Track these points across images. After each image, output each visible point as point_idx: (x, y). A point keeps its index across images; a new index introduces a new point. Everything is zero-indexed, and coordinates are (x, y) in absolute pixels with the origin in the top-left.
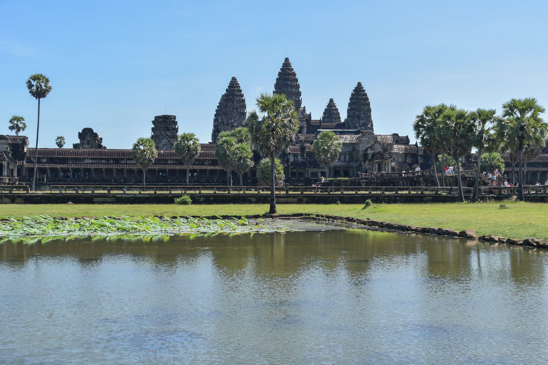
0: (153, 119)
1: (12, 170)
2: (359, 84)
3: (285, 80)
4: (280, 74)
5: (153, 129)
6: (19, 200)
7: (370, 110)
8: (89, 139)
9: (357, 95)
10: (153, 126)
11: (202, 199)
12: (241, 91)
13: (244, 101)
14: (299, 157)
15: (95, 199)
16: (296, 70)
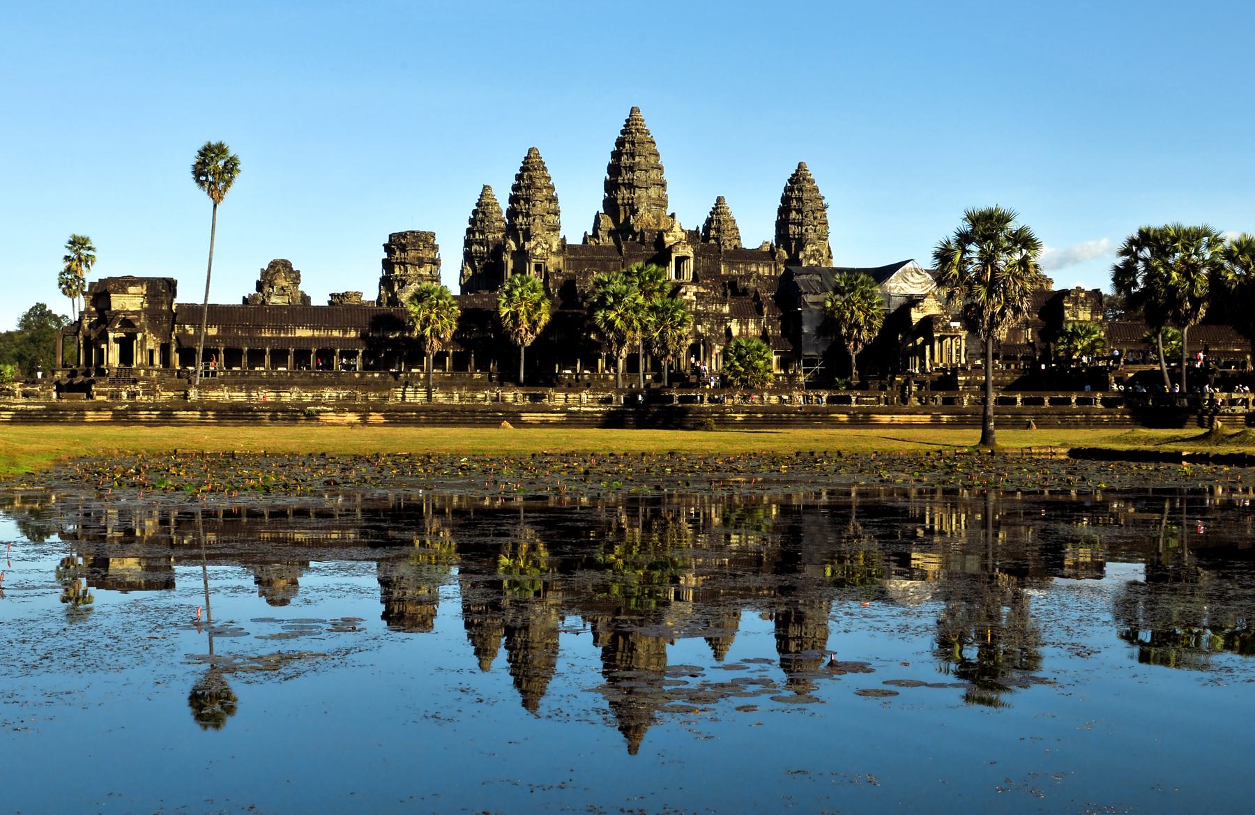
0: (387, 242)
1: (151, 352)
2: (801, 166)
3: (632, 155)
4: (620, 143)
5: (388, 265)
6: (375, 417)
7: (826, 223)
8: (284, 284)
9: (800, 190)
10: (385, 256)
11: (739, 417)
13: (554, 200)
14: (752, 326)
15: (526, 417)
16: (655, 134)
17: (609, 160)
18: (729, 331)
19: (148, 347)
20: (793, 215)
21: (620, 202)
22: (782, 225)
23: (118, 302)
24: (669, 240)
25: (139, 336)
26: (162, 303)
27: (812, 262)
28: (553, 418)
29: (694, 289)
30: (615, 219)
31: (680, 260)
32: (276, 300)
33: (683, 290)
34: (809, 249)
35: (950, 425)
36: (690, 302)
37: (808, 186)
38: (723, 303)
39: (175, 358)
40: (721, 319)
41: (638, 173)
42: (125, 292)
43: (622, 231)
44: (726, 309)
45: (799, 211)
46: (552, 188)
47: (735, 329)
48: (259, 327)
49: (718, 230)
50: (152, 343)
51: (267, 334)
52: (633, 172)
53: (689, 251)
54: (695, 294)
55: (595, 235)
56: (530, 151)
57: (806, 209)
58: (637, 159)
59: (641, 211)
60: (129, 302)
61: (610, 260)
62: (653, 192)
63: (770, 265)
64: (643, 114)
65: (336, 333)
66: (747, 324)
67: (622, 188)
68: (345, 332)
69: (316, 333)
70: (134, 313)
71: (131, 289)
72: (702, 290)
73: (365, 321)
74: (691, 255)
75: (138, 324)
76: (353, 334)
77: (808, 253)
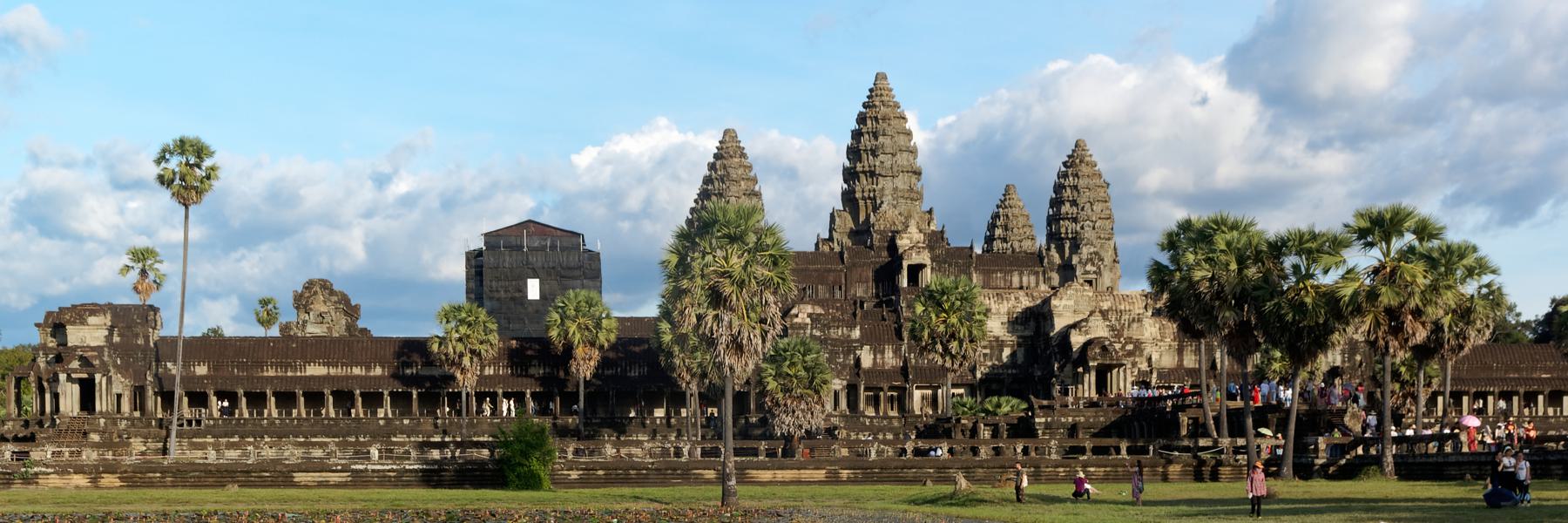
1: (119, 396)
3: (875, 135)
4: (861, 119)
6: (109, 480)
8: (323, 309)
11: (574, 475)
12: (750, 168)
15: (299, 477)
17: (848, 140)
18: (858, 361)
19: (117, 389)
20: (1066, 208)
21: (858, 195)
22: (1053, 220)
23: (75, 336)
24: (903, 243)
25: (98, 377)
26: (137, 336)
27: (1089, 267)
28: (334, 478)
29: (809, 309)
30: (855, 218)
31: (915, 270)
32: (314, 330)
33: (794, 311)
34: (1085, 251)
35: (850, 481)
36: (803, 326)
37: (1084, 169)
38: (852, 327)
39: (153, 402)
40: (849, 347)
41: (882, 157)
42: (83, 322)
43: (861, 233)
44: (856, 333)
45: (1074, 203)
46: (755, 180)
47: (867, 359)
48: (260, 365)
49: (1006, 228)
50: (121, 385)
51: (271, 373)
52: (875, 155)
53: (925, 257)
54: (810, 315)
55: (831, 239)
56: (726, 132)
57: (1081, 201)
58: (881, 139)
59: (884, 206)
60: (89, 335)
61: (830, 271)
62: (901, 182)
63: (1037, 274)
64: (893, 82)
65: (357, 371)
66: (883, 353)
67: (862, 177)
68: (368, 368)
69: (333, 371)
70: (93, 349)
71: (92, 320)
72: (819, 310)
73: (389, 352)
74: (928, 262)
75: (96, 362)
76: (378, 371)
77: (1084, 257)
